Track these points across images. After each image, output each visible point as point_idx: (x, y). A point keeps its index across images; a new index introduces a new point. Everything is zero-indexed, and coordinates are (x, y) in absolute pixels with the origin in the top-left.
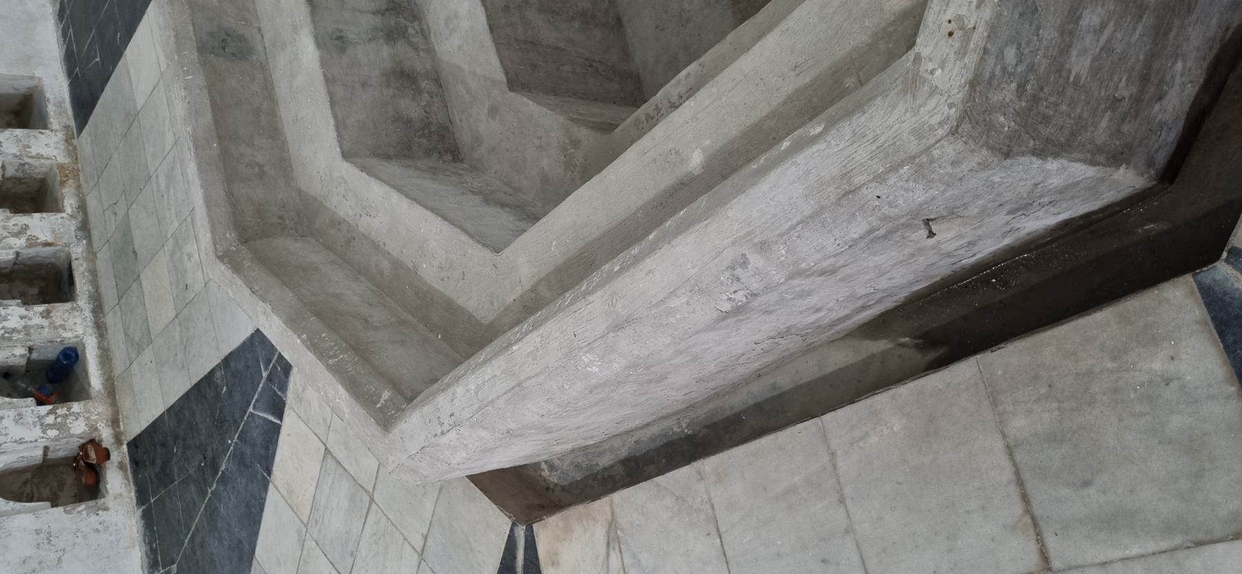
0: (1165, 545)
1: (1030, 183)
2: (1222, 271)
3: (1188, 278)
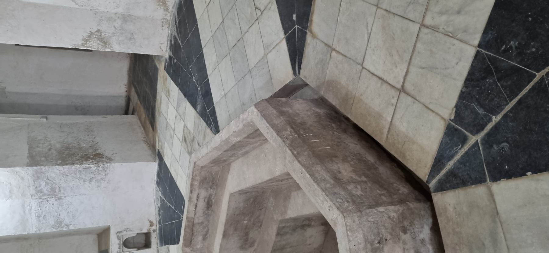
0: (499, 225)
1: (388, 220)
2: (432, 185)
3: (432, 194)
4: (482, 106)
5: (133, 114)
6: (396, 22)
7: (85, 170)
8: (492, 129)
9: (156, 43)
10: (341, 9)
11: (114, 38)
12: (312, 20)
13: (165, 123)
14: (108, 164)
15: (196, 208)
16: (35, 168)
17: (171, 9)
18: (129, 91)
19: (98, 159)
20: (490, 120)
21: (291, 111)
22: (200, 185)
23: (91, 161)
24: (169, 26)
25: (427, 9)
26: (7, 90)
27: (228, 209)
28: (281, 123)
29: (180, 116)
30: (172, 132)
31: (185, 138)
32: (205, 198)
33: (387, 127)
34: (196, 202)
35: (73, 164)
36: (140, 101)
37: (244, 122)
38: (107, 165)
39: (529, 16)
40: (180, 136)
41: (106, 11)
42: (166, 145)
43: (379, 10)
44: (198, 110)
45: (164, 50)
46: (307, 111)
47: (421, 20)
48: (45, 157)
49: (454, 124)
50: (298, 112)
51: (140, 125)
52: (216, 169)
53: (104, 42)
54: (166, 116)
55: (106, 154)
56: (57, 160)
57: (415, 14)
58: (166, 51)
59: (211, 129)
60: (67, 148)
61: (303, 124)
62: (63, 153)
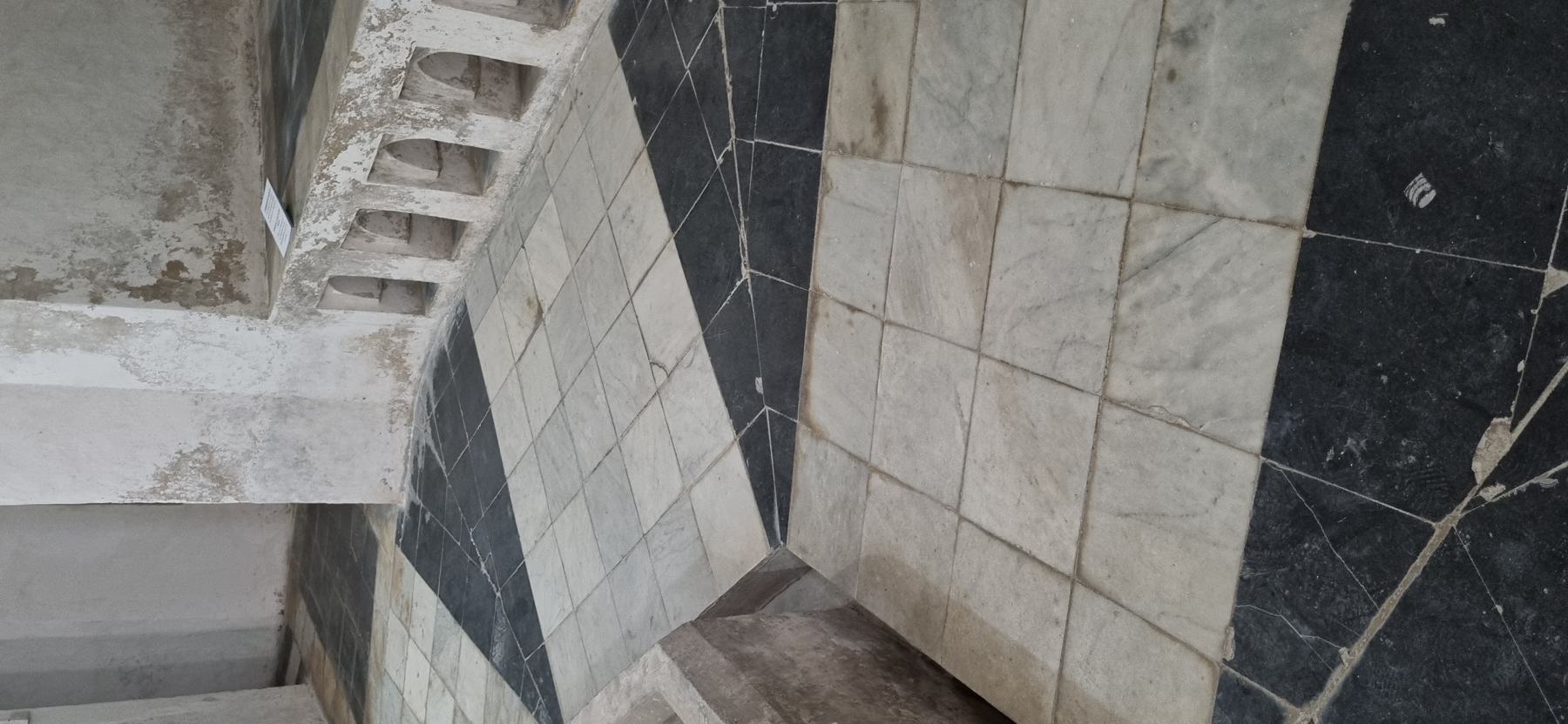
4: (1304, 619)
5: (298, 681)
6: (1034, 394)
8: (1345, 685)
9: (373, 471)
10: (884, 360)
11: (249, 464)
12: (806, 393)
13: (398, 706)
17: (415, 373)
18: (288, 613)
20: (1335, 661)
21: (768, 653)
24: (410, 421)
25: (1109, 358)
28: (741, 693)
29: (443, 681)
33: (1051, 687)
36: (321, 640)
37: (634, 695)
39: (1379, 372)
41: (228, 391)
43: (983, 362)
44: (496, 660)
46: (816, 649)
47: (1099, 386)
49: (1238, 675)
50: (789, 654)
54: (399, 682)
57: (1082, 371)
58: (402, 489)
59: (537, 716)
61: (806, 691)
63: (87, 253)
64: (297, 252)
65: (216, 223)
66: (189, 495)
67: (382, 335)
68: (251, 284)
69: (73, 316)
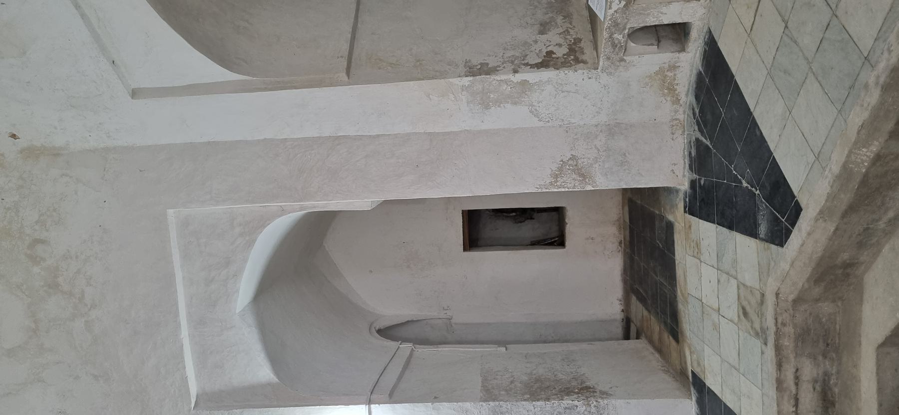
5: (637, 338)
7: (568, 411)
9: (668, 168)
11: (597, 165)
14: (606, 402)
15: (796, 405)
16: (492, 403)
18: (626, 310)
19: (588, 394)
22: (796, 346)
23: (576, 396)
24: (684, 131)
26: (453, 321)
27: (880, 390)
30: (715, 316)
31: (744, 309)
32: (815, 381)
34: (794, 392)
35: (548, 399)
36: (647, 309)
38: (603, 402)
40: (733, 312)
41: (582, 123)
42: (707, 351)
45: (680, 176)
48: (506, 391)
51: (653, 351)
52: (826, 308)
53: (583, 176)
55: (600, 388)
56: (523, 395)
58: (684, 176)
60: (537, 380)
62: (532, 387)
63: (510, 53)
64: (611, 12)
65: (567, 32)
66: (569, 185)
67: (661, 71)
68: (588, 54)
69: (506, 82)
